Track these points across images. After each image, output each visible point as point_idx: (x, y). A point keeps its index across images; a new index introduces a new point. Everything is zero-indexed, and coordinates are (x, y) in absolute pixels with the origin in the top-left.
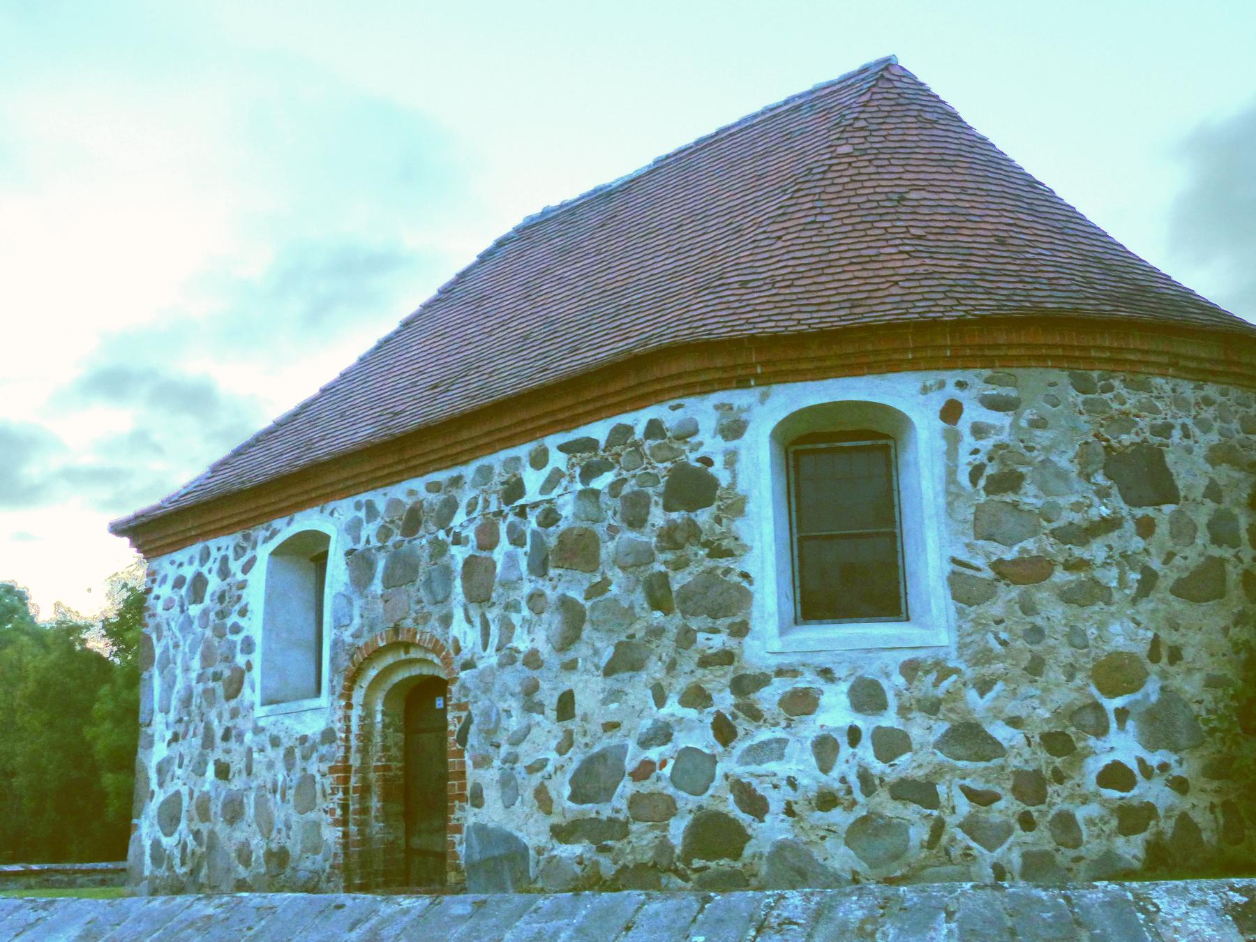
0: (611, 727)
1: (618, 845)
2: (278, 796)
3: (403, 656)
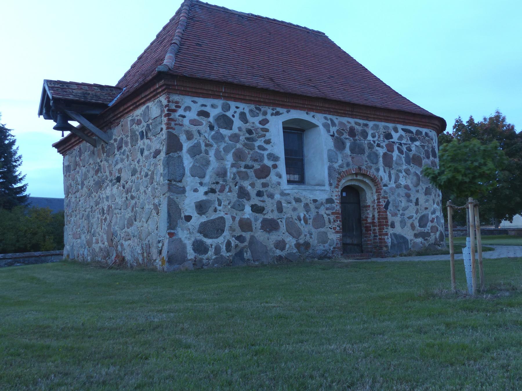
0: (426, 208)
1: (429, 238)
2: (302, 222)
3: (355, 178)
